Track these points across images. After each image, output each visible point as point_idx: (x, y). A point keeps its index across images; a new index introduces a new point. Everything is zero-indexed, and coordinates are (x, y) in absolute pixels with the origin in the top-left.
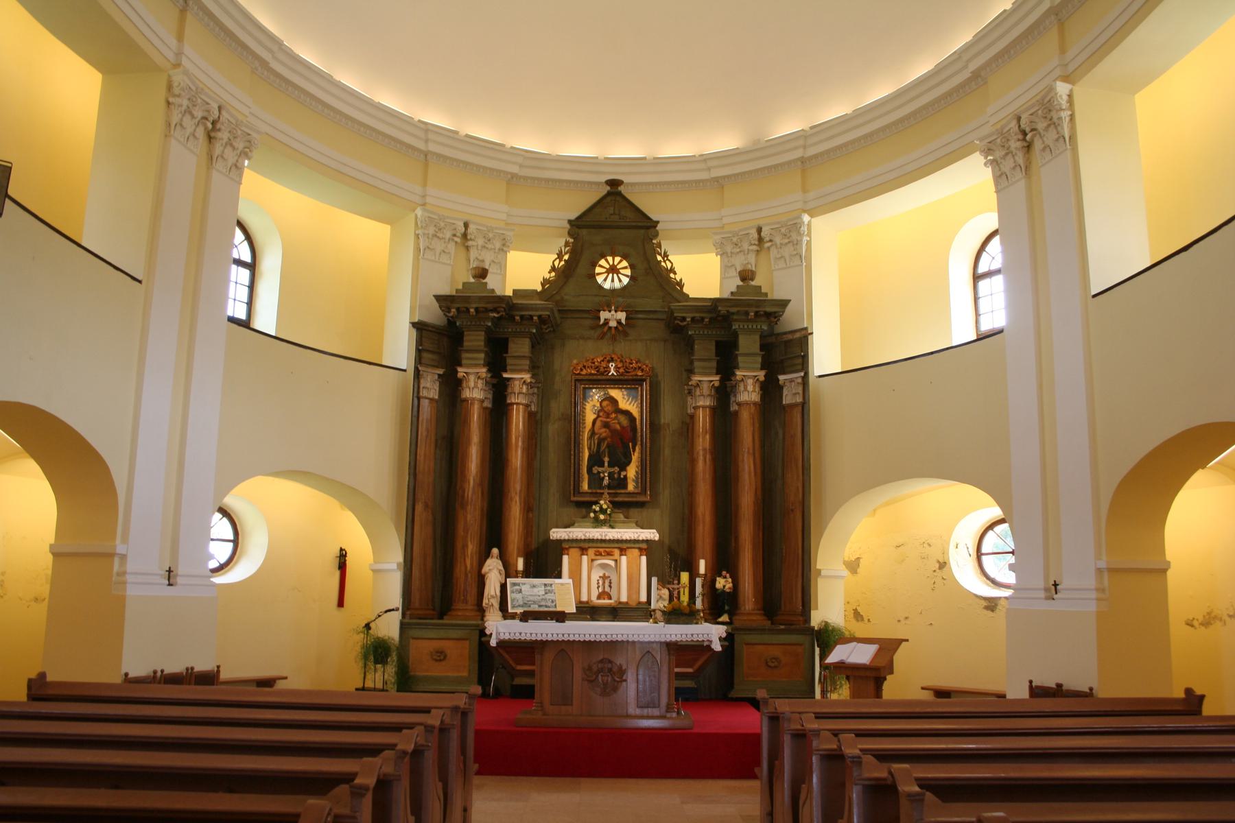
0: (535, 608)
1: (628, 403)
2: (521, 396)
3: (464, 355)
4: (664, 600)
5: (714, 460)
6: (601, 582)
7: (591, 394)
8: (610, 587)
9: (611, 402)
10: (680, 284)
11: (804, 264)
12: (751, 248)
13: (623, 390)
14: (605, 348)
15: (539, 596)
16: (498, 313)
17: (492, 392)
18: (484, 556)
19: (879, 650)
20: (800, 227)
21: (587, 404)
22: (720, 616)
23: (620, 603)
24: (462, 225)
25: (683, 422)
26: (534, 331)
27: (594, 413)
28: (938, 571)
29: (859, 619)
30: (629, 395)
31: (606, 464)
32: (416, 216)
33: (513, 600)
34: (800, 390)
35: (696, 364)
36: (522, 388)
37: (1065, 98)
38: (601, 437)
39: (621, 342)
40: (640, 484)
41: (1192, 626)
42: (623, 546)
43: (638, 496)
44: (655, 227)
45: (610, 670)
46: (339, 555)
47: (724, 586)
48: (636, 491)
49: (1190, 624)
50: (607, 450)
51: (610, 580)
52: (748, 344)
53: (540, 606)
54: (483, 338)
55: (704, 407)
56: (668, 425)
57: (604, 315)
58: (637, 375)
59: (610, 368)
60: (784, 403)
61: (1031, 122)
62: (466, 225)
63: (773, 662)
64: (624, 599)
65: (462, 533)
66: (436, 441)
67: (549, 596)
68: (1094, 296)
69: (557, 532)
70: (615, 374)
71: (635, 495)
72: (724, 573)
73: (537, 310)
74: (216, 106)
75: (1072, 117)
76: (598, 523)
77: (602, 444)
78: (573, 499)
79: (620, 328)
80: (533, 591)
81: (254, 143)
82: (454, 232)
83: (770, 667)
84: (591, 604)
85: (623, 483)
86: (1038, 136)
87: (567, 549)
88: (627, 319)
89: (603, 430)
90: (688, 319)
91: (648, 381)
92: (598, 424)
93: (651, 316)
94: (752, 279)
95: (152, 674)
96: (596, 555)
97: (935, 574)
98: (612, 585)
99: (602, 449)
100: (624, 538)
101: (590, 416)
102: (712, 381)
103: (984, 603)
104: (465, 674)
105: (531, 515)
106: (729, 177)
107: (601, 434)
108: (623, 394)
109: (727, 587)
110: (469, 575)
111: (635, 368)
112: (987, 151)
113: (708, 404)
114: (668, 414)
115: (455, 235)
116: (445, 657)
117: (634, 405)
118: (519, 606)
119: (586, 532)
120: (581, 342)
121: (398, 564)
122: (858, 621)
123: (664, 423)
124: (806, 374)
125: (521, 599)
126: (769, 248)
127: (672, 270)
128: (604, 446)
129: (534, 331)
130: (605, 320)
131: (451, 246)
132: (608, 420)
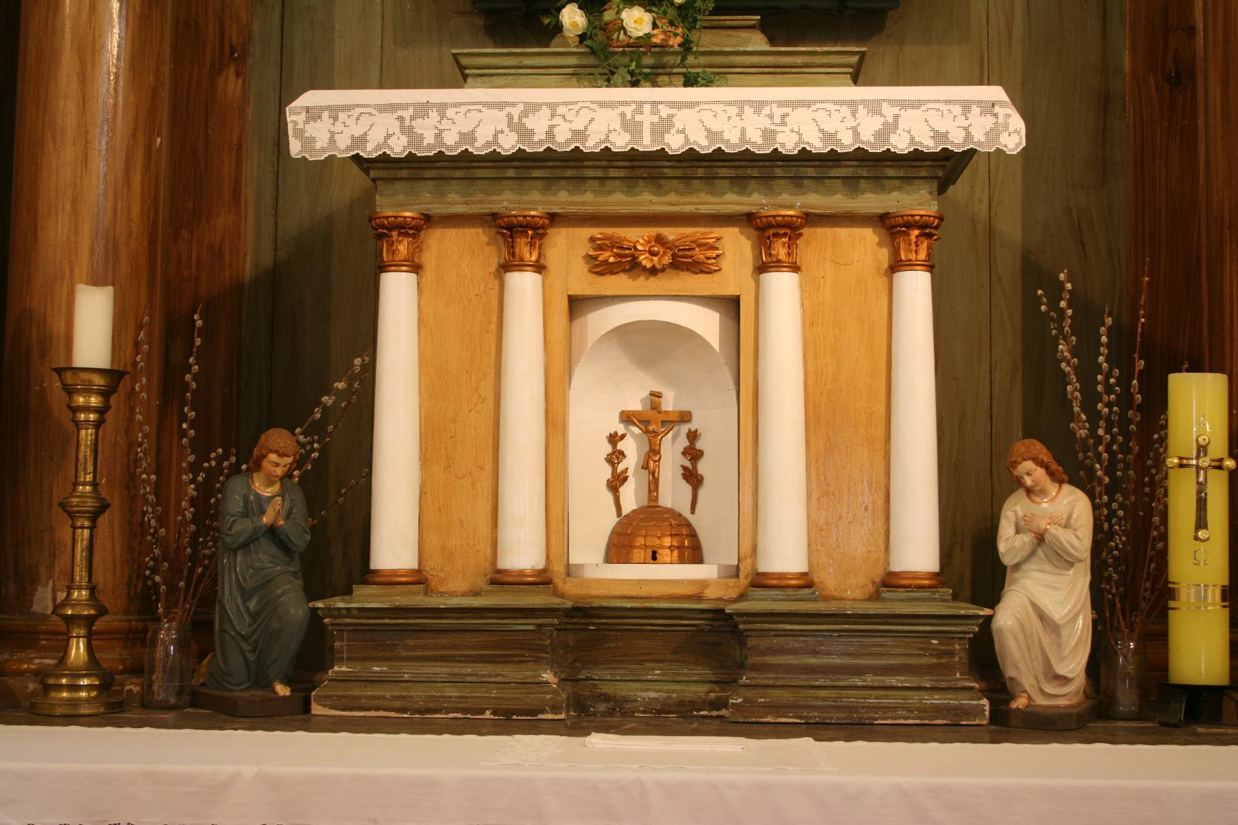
4: (1063, 560)
6: (631, 448)
8: (693, 478)
23: (761, 581)
51: (693, 436)
69: (335, 111)
84: (570, 588)
87: (414, 230)
96: (601, 269)
98: (703, 467)
100: (788, 143)
105: (231, 85)
119: (531, 108)
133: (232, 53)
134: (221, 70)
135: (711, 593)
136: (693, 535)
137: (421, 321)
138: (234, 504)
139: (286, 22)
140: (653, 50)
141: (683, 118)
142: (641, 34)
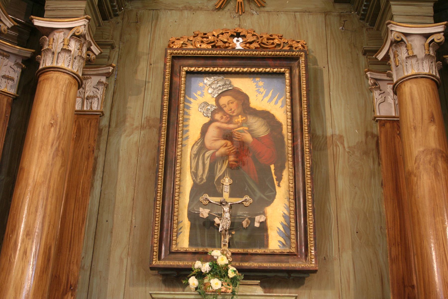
1: (267, 99)
2: (64, 55)
7: (201, 84)
17: (19, 70)
21: (192, 100)
25: (367, 134)
31: (227, 190)
39: (253, 14)
40: (293, 237)
43: (290, 260)
48: (287, 250)
56: (341, 137)
59: (235, 44)
71: (283, 258)
77: (219, 166)
78: (156, 263)
89: (223, 142)
91: (302, 60)
92: (212, 132)
99: (219, 174)
108: (257, 86)
113: (427, 71)
117: (276, 103)
120: (186, 13)
132: (231, 126)
133: (70, 288)
134: (66, 293)
139: (91, 276)
140: (221, 293)
142: (217, 288)
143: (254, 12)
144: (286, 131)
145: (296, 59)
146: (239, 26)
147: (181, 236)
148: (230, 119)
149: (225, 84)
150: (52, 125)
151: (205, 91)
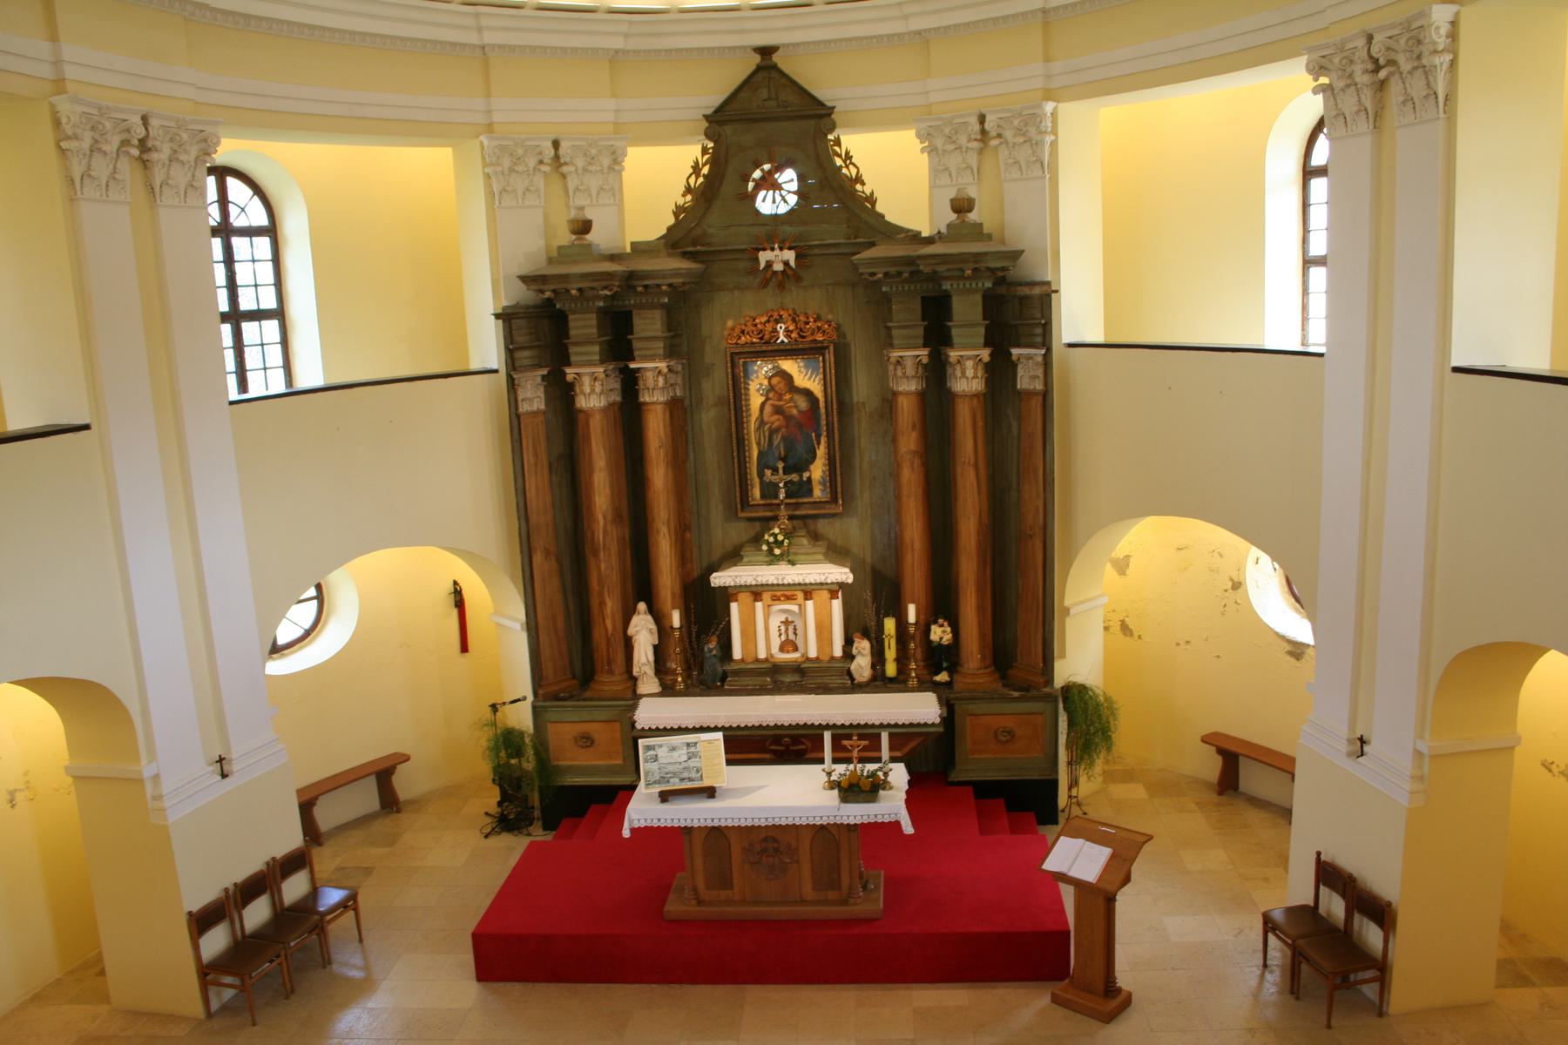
0: (675, 784)
3: (572, 350)
5: (926, 465)
6: (783, 628)
7: (756, 368)
8: (795, 634)
9: (783, 378)
10: (871, 199)
11: (1048, 176)
12: (970, 145)
13: (799, 360)
14: (770, 299)
15: (680, 763)
16: (611, 290)
17: (619, 380)
18: (628, 614)
19: (1113, 857)
20: (1041, 122)
21: (750, 382)
22: (937, 674)
23: (808, 659)
24: (549, 144)
26: (666, 300)
27: (762, 395)
28: (1230, 591)
29: (1128, 633)
30: (807, 367)
31: (781, 471)
32: (482, 143)
33: (647, 774)
34: (1040, 372)
35: (895, 333)
36: (657, 381)
37: (1445, 29)
38: (773, 427)
39: (791, 291)
41: (1550, 771)
42: (808, 591)
43: (827, 506)
44: (829, 115)
45: (776, 850)
46: (453, 590)
47: (941, 639)
49: (1547, 766)
50: (782, 445)
51: (795, 626)
52: (966, 309)
53: (682, 780)
54: (594, 322)
55: (907, 394)
56: (863, 404)
57: (764, 257)
58: (815, 341)
59: (778, 332)
60: (1019, 387)
61: (1388, 49)
62: (556, 144)
63: (1005, 736)
64: (813, 653)
65: (597, 588)
66: (550, 465)
67: (694, 763)
68: (1456, 370)
70: (786, 341)
71: (823, 505)
72: (941, 621)
73: (664, 277)
74: (137, 120)
75: (1453, 64)
76: (772, 559)
77: (775, 437)
79: (789, 272)
80: (672, 757)
81: (211, 142)
82: (540, 157)
83: (1001, 741)
85: (806, 488)
86: (1397, 75)
87: (736, 594)
88: (797, 257)
89: (776, 417)
90: (880, 276)
92: (768, 409)
93: (833, 251)
94: (970, 210)
95: (224, 894)
97: (1227, 594)
98: (797, 632)
99: (776, 443)
100: (807, 581)
101: (756, 401)
102: (919, 356)
103: (1288, 647)
104: (619, 762)
105: (688, 535)
106: (937, 29)
107: (772, 423)
108: (799, 367)
109: (944, 639)
110: (612, 640)
111: (813, 330)
112: (1317, 69)
114: (862, 388)
115: (541, 162)
116: (593, 742)
117: (814, 381)
118: (655, 782)
119: (758, 576)
120: (736, 293)
121: (522, 625)
122: (1125, 634)
123: (858, 403)
124: (1049, 350)
125: (658, 771)
126: (996, 147)
127: (859, 179)
128: (777, 439)
129: (666, 300)
130: (767, 262)
131: (539, 181)
132: (781, 403)
135: (799, 660)
136: (796, 646)
137: (739, 612)
138: (706, 649)
141: (787, 577)
143: (793, 288)
144: (822, 404)
145: (827, 347)
146: (782, 303)
147: (754, 490)
148: (780, 399)
149: (774, 368)
150: (660, 447)
151: (760, 375)
